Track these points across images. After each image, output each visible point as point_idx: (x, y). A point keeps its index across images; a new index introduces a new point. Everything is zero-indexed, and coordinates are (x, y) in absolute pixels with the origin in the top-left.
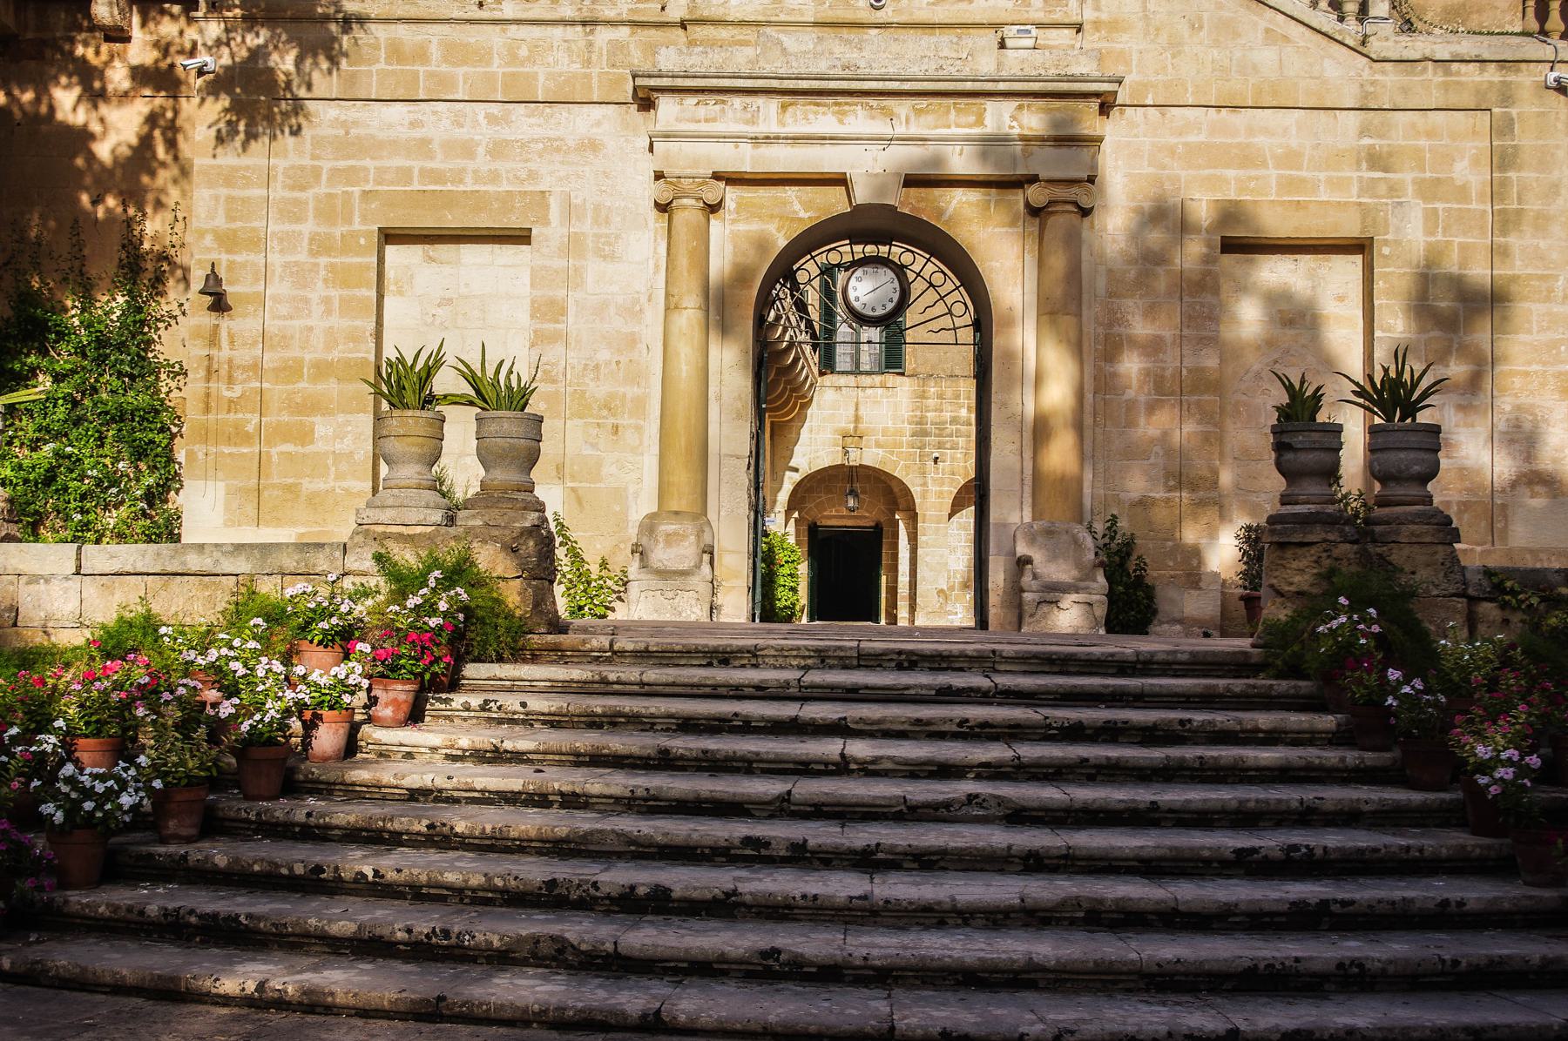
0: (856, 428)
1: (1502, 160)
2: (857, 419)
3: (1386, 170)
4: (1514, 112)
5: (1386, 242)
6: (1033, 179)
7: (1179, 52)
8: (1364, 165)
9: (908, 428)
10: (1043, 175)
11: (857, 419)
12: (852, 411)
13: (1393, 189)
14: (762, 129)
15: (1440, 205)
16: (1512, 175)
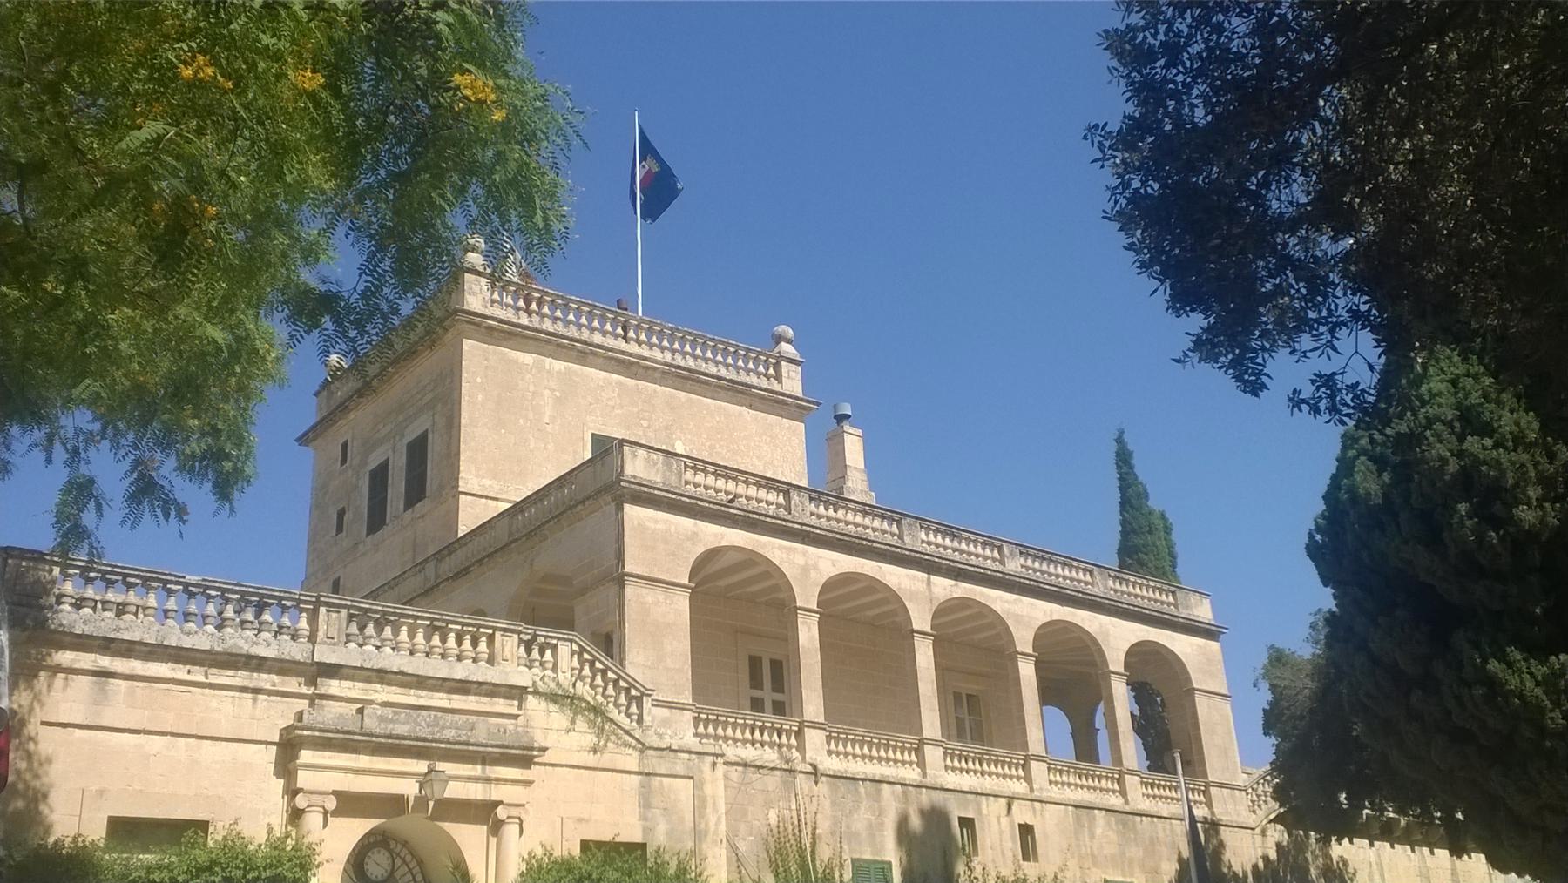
6: (501, 803)
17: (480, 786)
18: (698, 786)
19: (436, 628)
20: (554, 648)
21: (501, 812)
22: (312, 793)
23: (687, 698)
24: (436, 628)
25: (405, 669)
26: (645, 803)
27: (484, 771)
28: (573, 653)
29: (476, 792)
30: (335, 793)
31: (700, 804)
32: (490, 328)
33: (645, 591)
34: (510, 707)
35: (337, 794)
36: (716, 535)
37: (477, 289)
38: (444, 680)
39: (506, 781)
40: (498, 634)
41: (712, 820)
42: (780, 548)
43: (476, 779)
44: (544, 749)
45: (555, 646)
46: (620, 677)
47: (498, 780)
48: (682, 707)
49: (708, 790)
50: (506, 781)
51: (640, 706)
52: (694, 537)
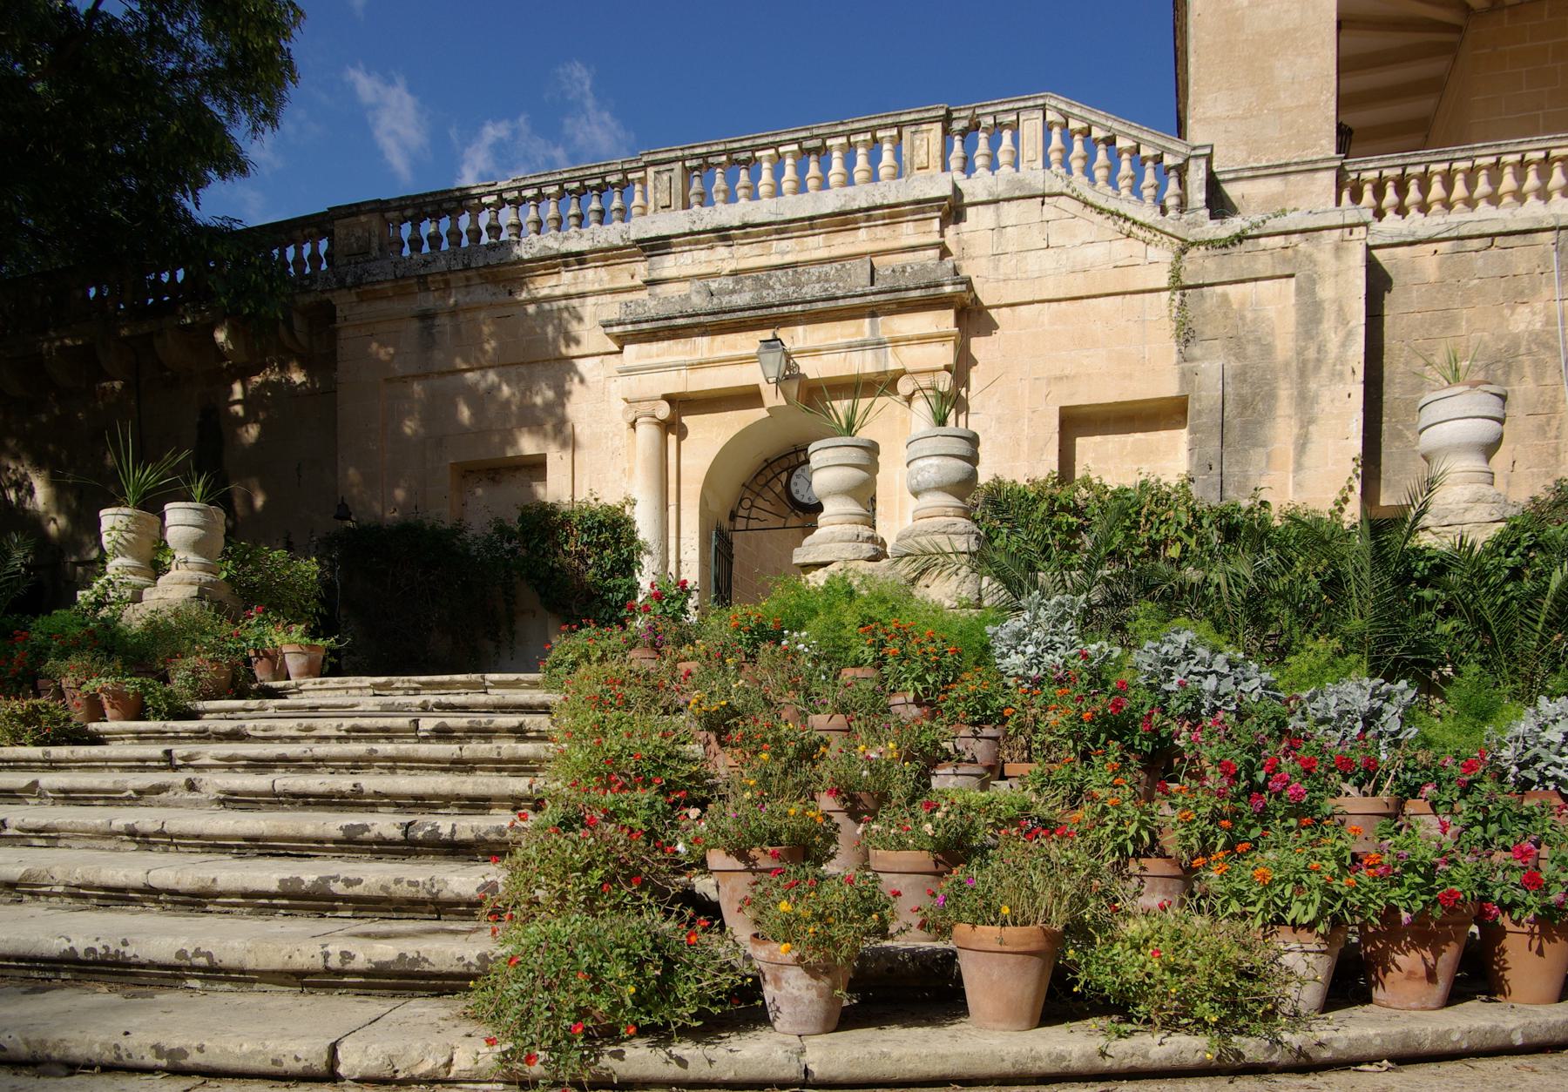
6: (903, 372)
10: (909, 369)
14: (697, 357)
17: (869, 354)
18: (1307, 291)
20: (1015, 127)
21: (904, 386)
25: (750, 219)
26: (1186, 335)
27: (874, 329)
28: (1048, 128)
29: (864, 364)
31: (1310, 314)
34: (930, 230)
38: (811, 218)
39: (908, 340)
41: (1333, 341)
43: (863, 346)
47: (896, 342)
48: (1312, 168)
49: (1326, 292)
50: (908, 340)
51: (1182, 183)
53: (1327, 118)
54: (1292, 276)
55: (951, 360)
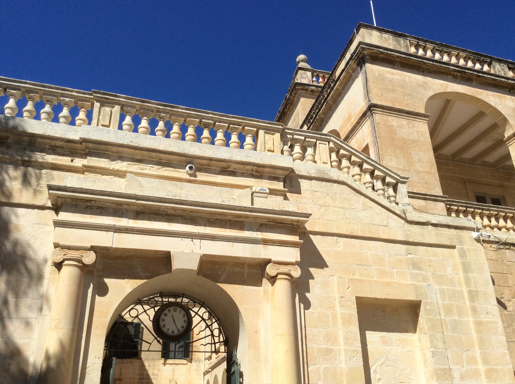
0: (120, 377)
1: (466, 268)
2: (121, 374)
3: (420, 270)
4: (465, 248)
5: (427, 303)
6: (269, 261)
7: (328, 209)
8: (411, 267)
9: (137, 377)
10: (273, 259)
11: (121, 374)
12: (119, 372)
13: (425, 279)
15: (445, 287)
16: (469, 274)
19: (206, 126)
21: (271, 270)
22: (69, 248)
23: (438, 191)
24: (206, 126)
28: (331, 150)
30: (93, 248)
32: (312, 91)
33: (390, 118)
35: (100, 252)
36: (441, 85)
37: (305, 76)
40: (261, 132)
42: (493, 95)
44: (308, 216)
45: (315, 145)
46: (376, 168)
48: (435, 199)
52: (424, 86)
53: (436, 179)
54: (454, 247)
55: (299, 260)
